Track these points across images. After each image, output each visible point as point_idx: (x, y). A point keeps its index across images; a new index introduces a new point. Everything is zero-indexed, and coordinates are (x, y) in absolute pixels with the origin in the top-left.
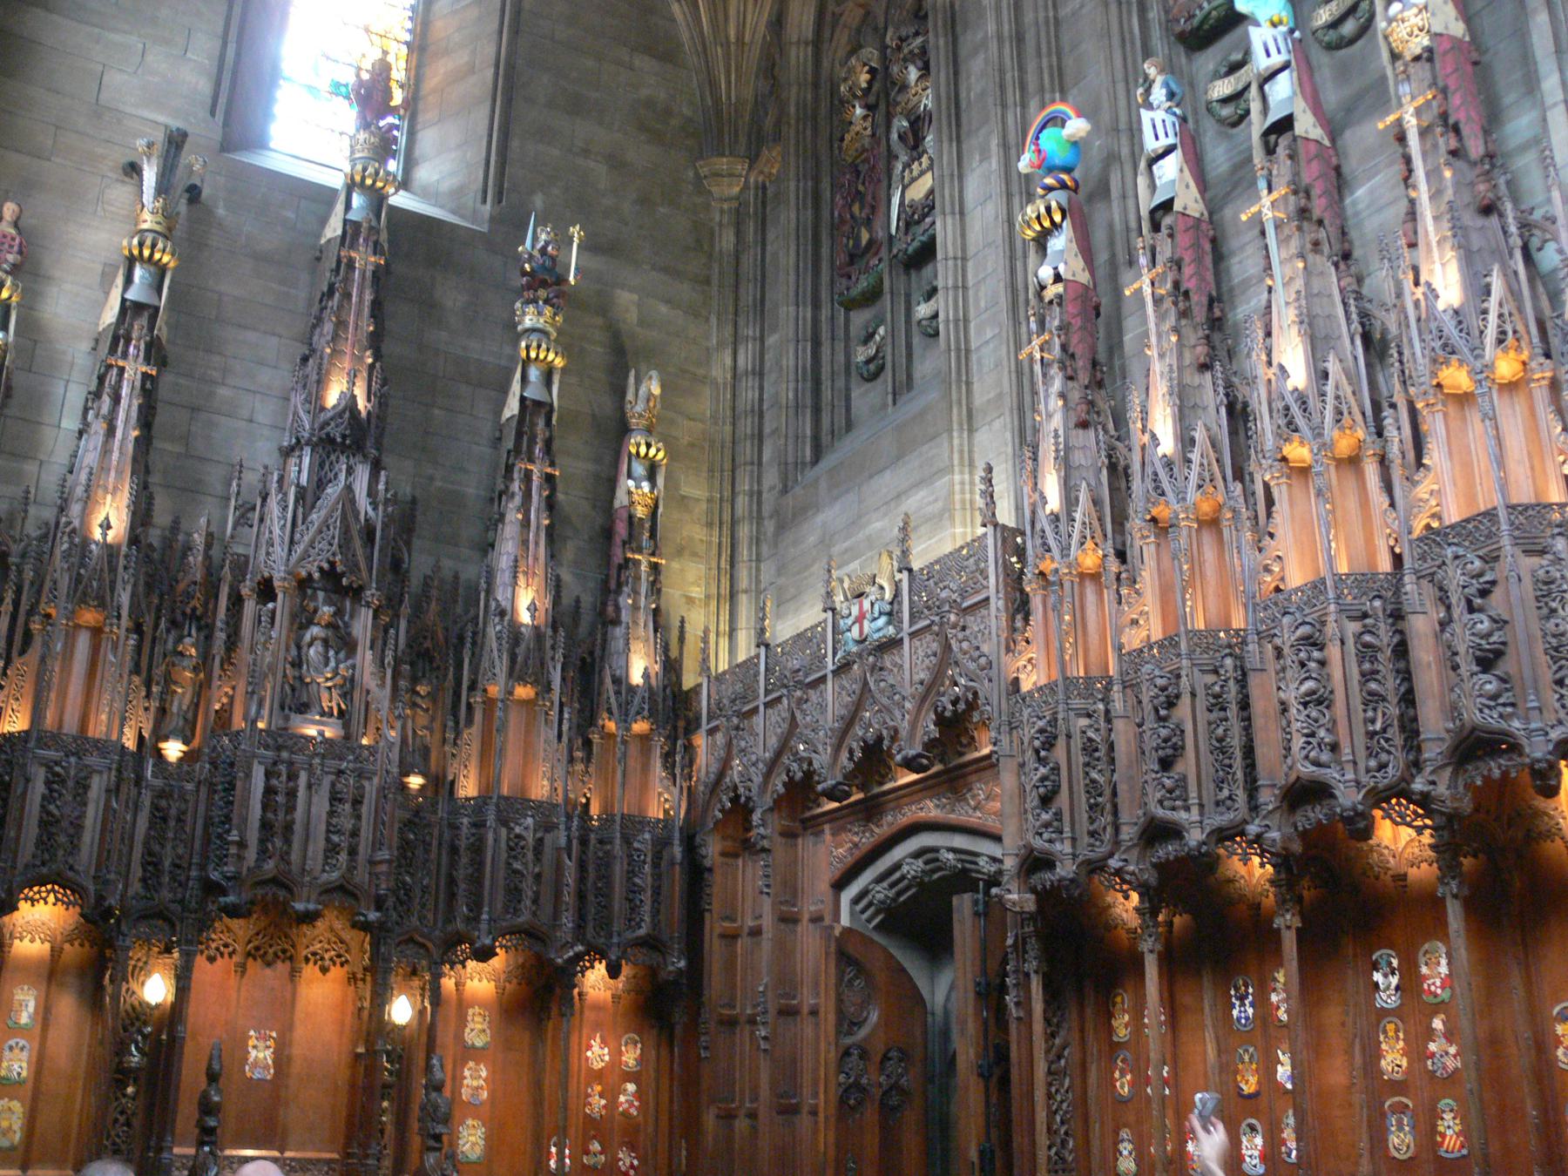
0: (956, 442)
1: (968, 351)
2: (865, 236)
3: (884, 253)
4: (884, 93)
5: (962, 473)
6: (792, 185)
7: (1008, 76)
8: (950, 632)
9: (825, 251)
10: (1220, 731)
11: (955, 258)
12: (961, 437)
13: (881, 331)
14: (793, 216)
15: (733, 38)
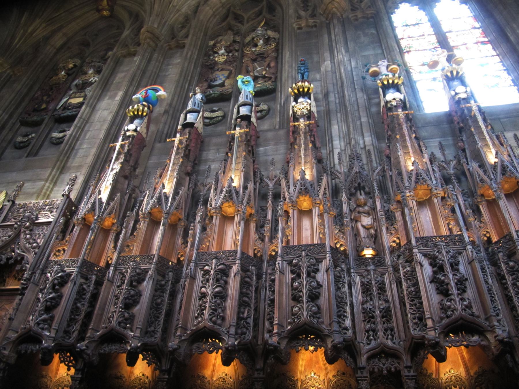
0: (53, 173)
1: (73, 148)
2: (44, 106)
3: (50, 113)
4: (76, 72)
5: (50, 184)
6: (25, 79)
7: (136, 78)
8: (23, 229)
9: (24, 104)
10: (159, 301)
11: (84, 120)
12: (56, 172)
13: (33, 135)
14: (19, 87)
15: (29, 31)
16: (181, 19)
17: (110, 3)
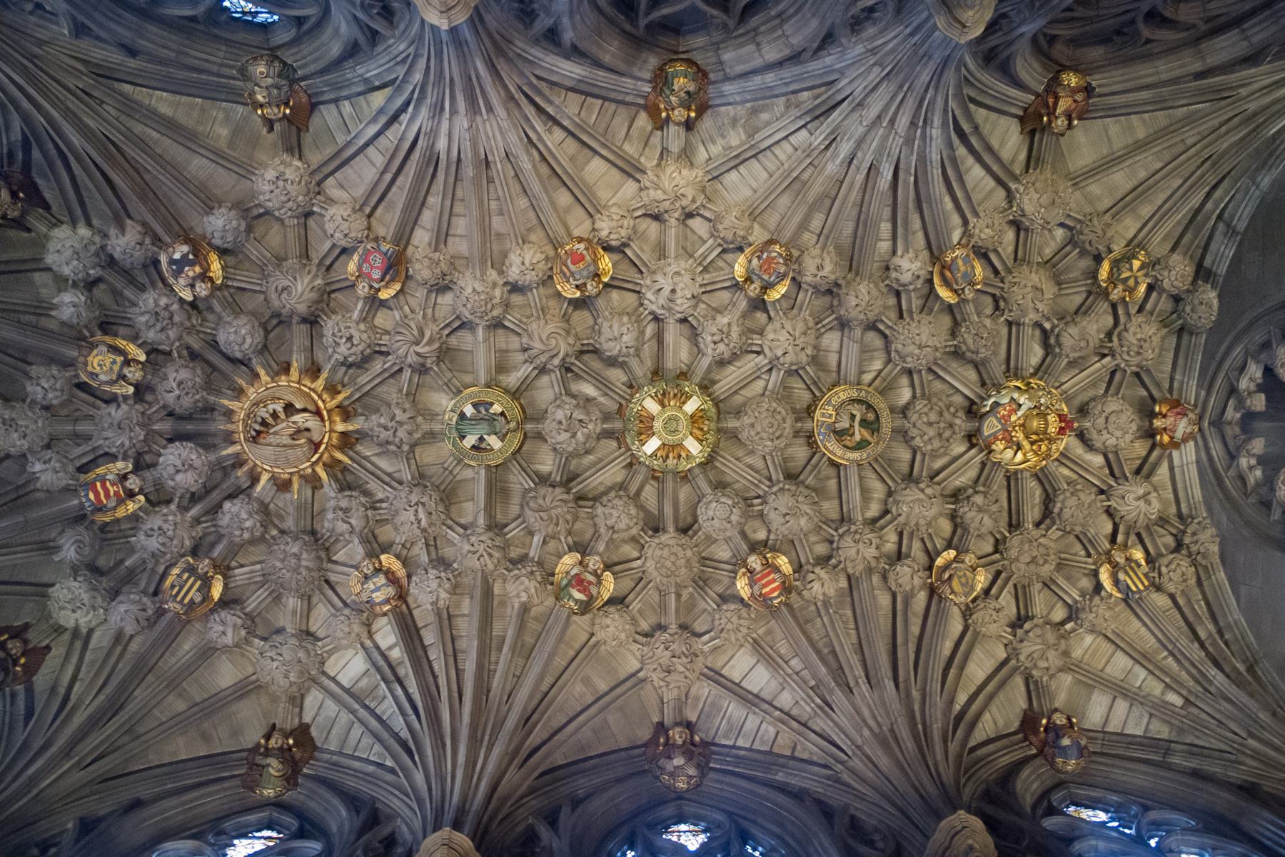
16: (871, 31)
17: (1051, 101)
